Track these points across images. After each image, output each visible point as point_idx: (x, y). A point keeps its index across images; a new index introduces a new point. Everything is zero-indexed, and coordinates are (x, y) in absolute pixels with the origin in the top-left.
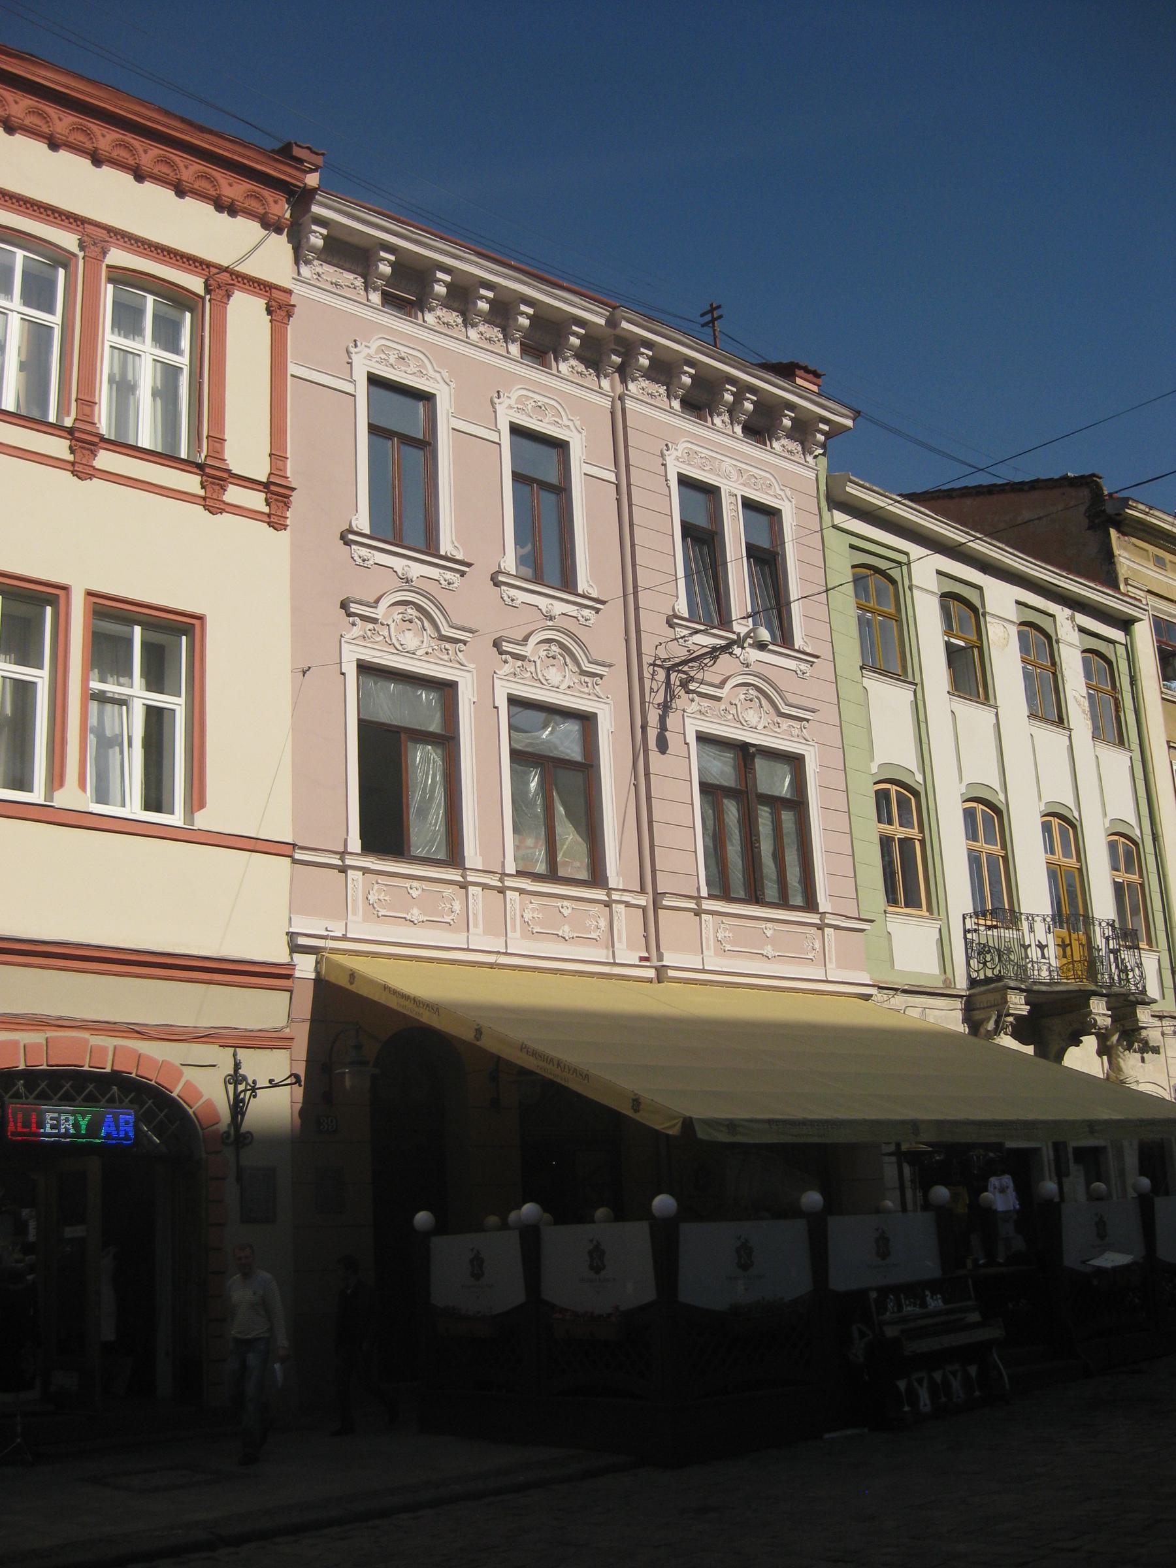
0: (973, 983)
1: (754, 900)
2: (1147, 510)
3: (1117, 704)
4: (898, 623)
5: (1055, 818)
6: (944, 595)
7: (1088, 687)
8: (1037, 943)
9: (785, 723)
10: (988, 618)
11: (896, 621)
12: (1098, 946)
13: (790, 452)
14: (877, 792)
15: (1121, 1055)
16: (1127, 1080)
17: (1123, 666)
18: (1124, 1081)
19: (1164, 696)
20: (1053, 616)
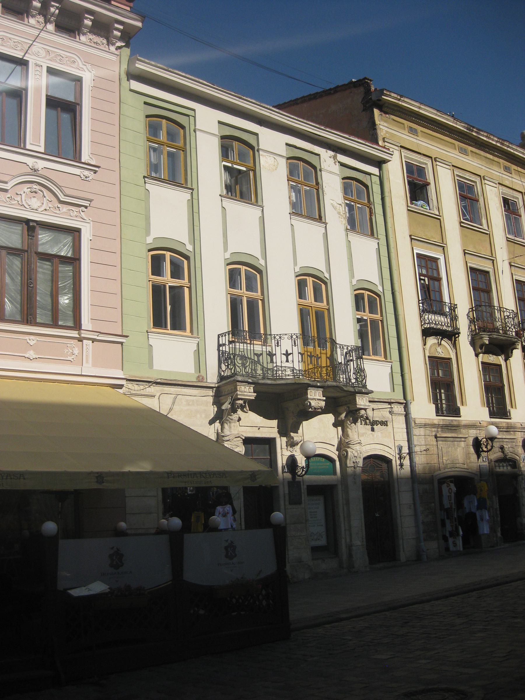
0: (222, 378)
1: (25, 321)
2: (399, 97)
3: (371, 211)
4: (185, 152)
5: (310, 277)
6: (223, 138)
7: (345, 199)
8: (268, 353)
9: (65, 208)
10: (261, 152)
11: (183, 151)
12: (318, 355)
13: (96, 43)
14: (153, 256)
15: (349, 426)
16: (351, 442)
17: (376, 189)
18: (349, 443)
19: (409, 208)
20: (318, 155)
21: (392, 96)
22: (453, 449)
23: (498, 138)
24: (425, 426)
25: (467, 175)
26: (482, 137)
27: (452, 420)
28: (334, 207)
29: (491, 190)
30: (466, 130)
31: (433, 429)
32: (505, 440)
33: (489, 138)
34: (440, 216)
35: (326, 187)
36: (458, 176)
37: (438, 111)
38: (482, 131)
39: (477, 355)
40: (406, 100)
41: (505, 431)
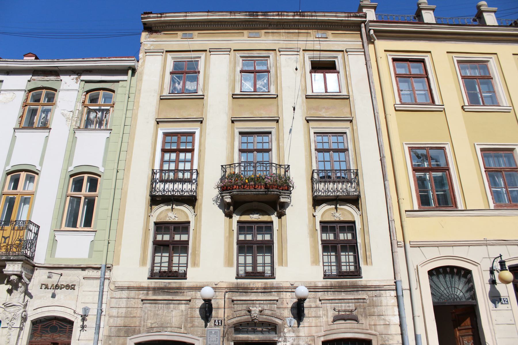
2: (160, 15)
19: (161, 97)
21: (151, 16)
22: (165, 312)
23: (294, 13)
24: (129, 288)
25: (255, 54)
26: (272, 17)
27: (169, 283)
28: (63, 115)
29: (289, 59)
30: (249, 17)
31: (142, 292)
32: (257, 302)
33: (281, 15)
34: (204, 95)
35: (59, 102)
36: (241, 57)
37: (208, 12)
38: (270, 12)
39: (229, 215)
40: (167, 15)
41: (261, 292)
